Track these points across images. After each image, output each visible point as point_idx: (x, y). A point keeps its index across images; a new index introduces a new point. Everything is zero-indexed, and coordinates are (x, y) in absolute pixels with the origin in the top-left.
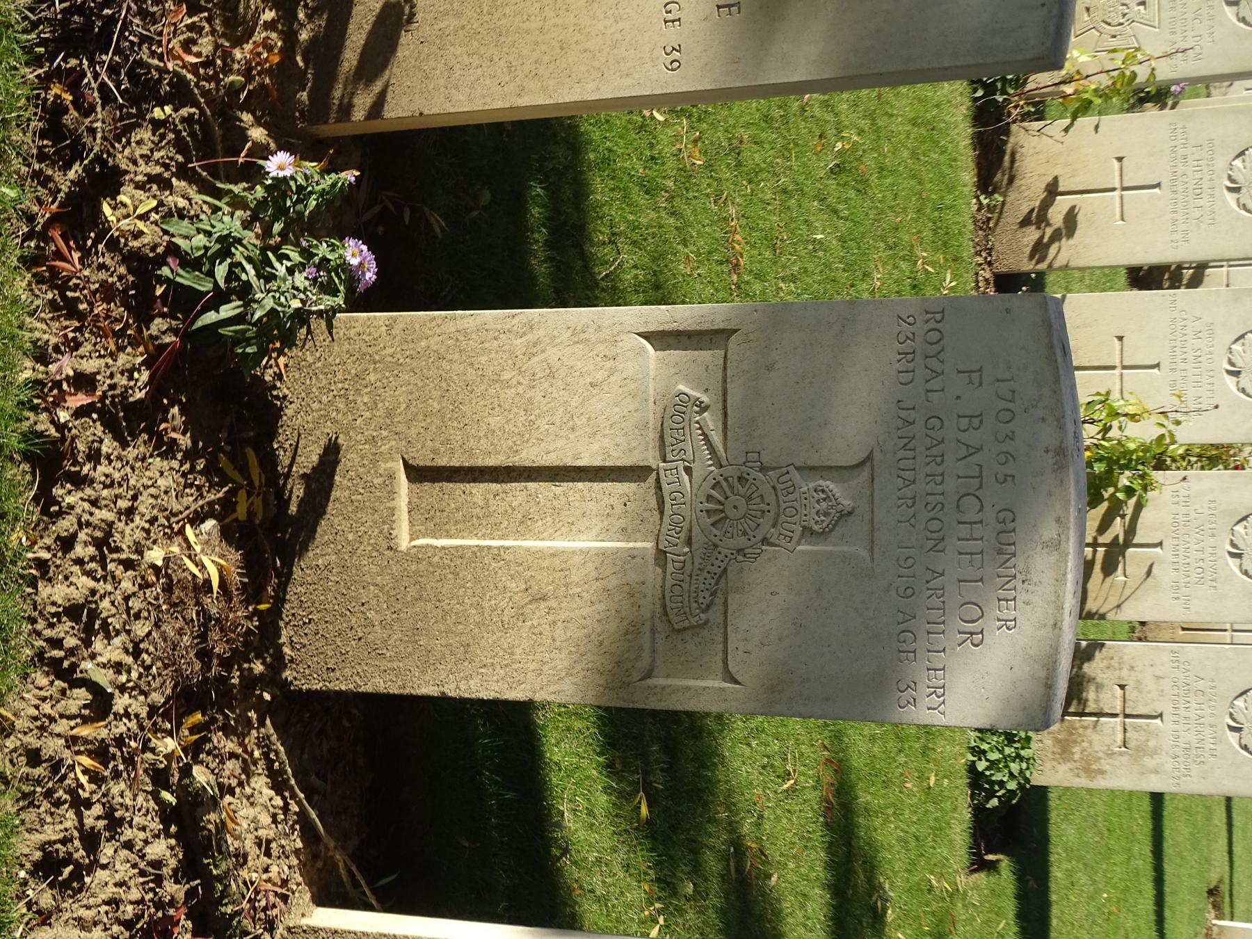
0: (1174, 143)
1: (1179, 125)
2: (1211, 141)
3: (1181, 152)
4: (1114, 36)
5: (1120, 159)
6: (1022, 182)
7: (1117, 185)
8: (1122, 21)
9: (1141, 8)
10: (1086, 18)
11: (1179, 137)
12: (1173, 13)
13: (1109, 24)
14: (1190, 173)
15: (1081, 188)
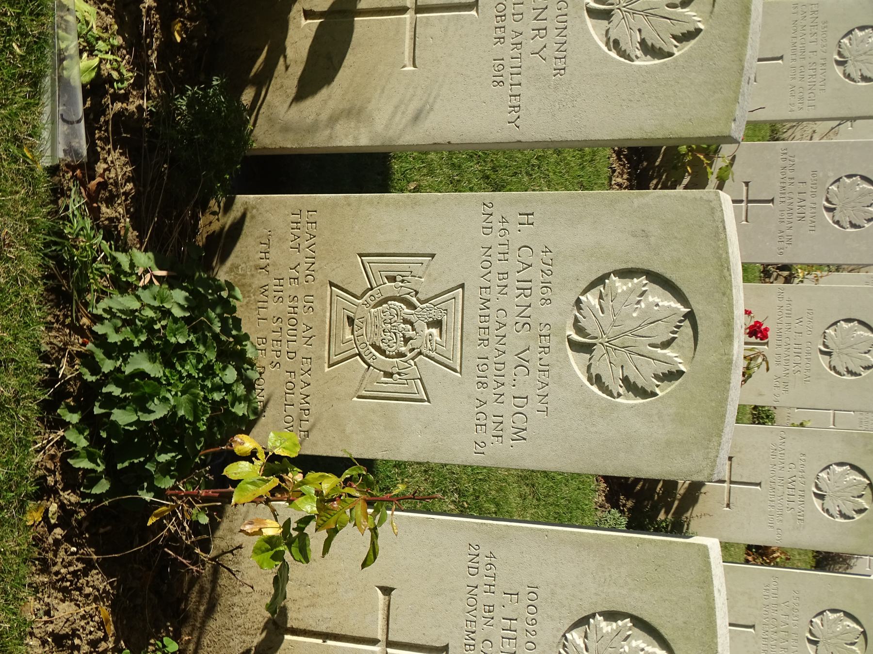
0: (473, 580)
1: (484, 551)
2: (533, 589)
3: (484, 598)
4: (390, 375)
5: (387, 591)
6: (236, 599)
7: (380, 636)
8: (403, 349)
9: (435, 331)
10: (349, 336)
11: (482, 571)
12: (483, 350)
13: (383, 352)
14: (497, 640)
15: (322, 628)
